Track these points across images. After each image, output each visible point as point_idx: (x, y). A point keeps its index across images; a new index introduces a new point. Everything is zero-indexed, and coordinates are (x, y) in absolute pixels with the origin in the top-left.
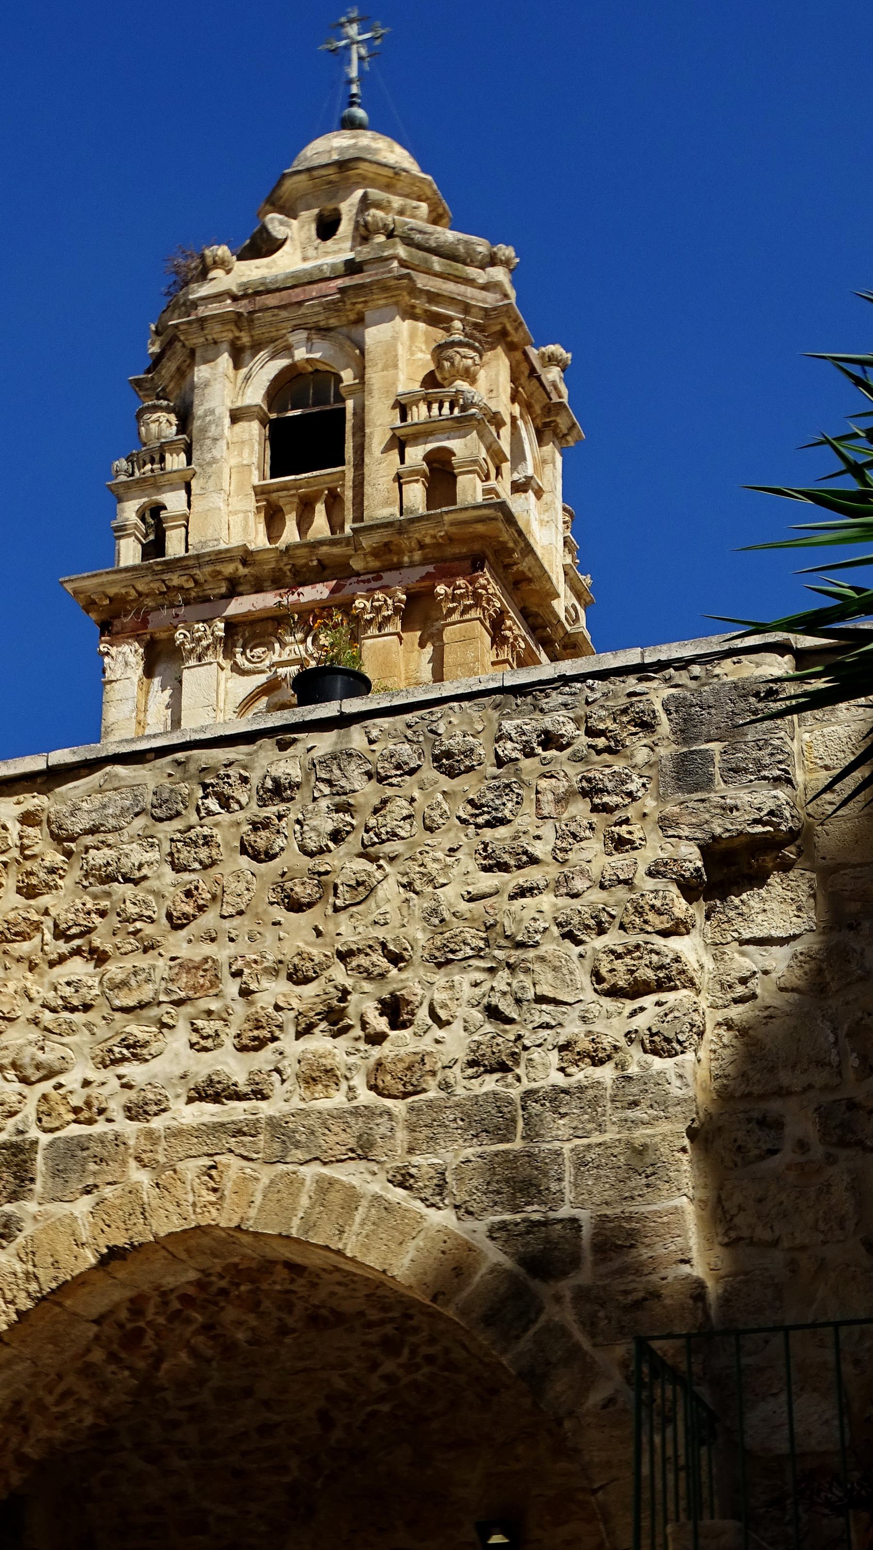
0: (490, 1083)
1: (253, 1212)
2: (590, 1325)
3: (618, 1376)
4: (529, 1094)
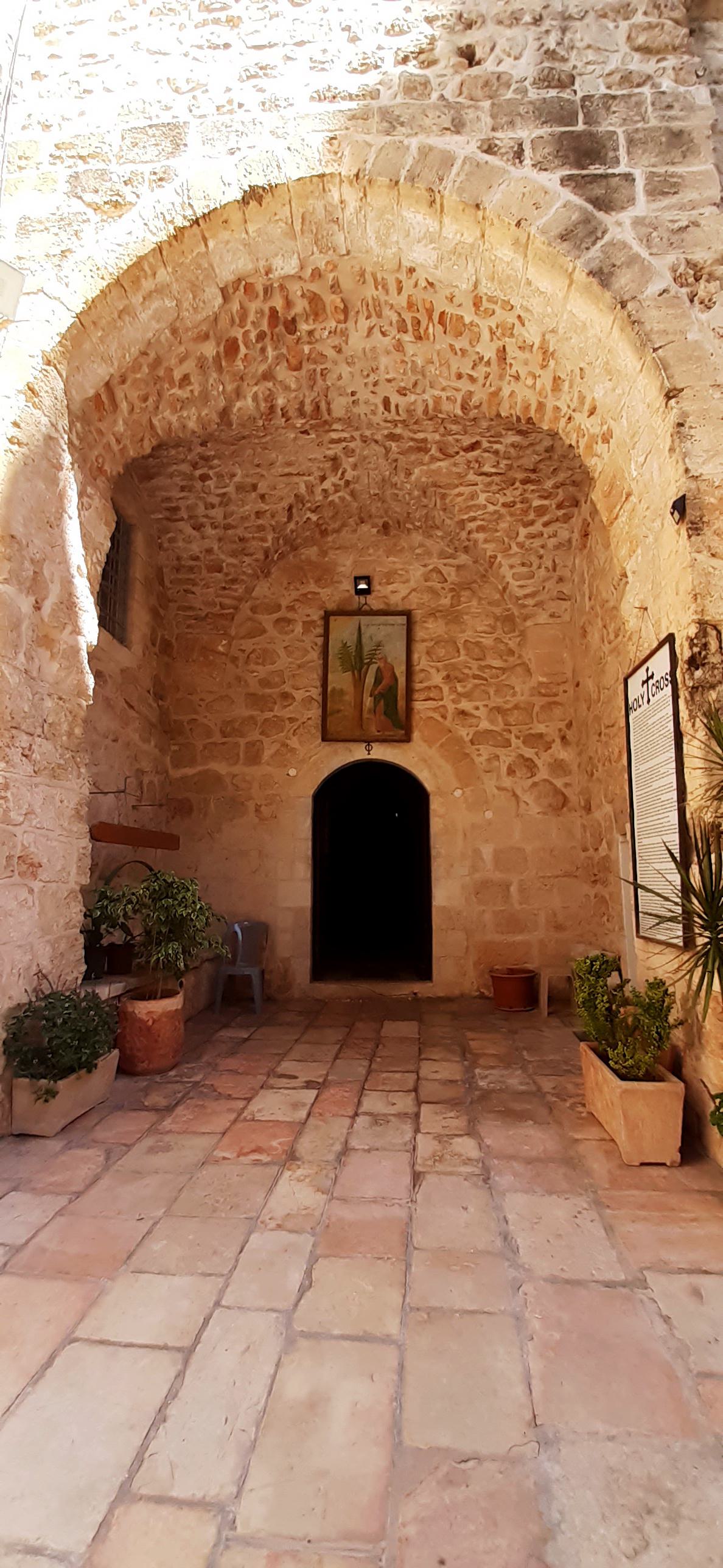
0: (553, 93)
1: (369, 166)
2: (648, 241)
3: (669, 276)
4: (585, 98)
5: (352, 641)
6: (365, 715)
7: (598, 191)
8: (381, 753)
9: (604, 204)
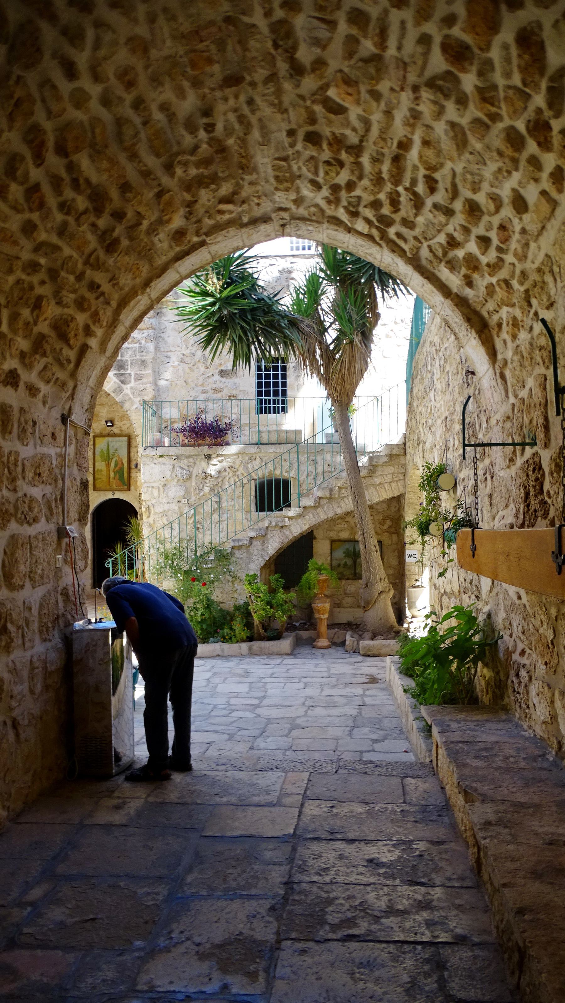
2: (133, 394)
3: (138, 404)
5: (105, 449)
6: (111, 480)
7: (122, 378)
8: (118, 495)
9: (123, 382)
